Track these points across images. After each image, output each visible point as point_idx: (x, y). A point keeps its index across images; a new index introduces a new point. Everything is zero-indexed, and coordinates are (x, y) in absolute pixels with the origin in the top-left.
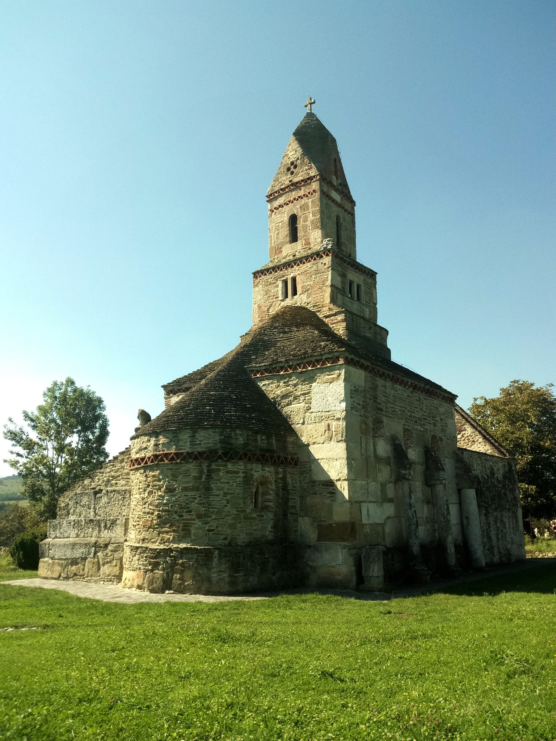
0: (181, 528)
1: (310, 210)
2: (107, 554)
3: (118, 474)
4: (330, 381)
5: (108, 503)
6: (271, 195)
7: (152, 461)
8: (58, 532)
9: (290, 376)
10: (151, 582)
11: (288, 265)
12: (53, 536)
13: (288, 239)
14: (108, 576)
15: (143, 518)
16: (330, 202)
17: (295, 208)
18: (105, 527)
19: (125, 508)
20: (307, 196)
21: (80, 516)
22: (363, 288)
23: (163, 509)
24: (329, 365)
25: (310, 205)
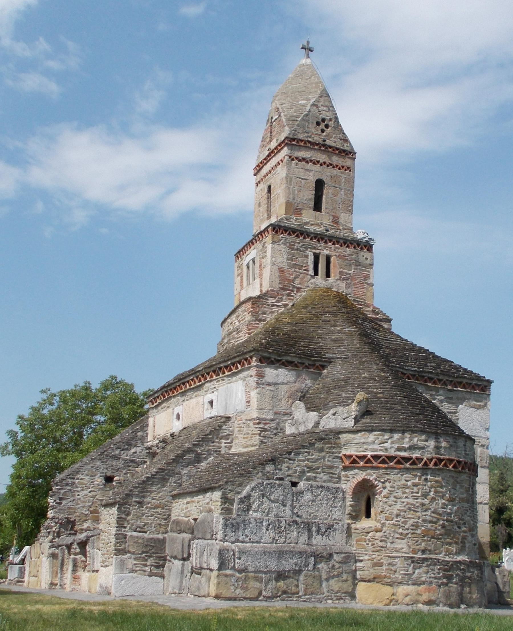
0: (460, 540)
2: (333, 566)
3: (316, 465)
4: (478, 407)
5: (313, 501)
6: (294, 140)
7: (436, 464)
8: (240, 533)
9: (437, 390)
10: (448, 596)
12: (233, 539)
14: (337, 593)
15: (422, 526)
17: (326, 174)
18: (318, 531)
19: (335, 510)
20: (339, 169)
21: (268, 514)
23: (447, 518)
24: (459, 389)
25: (343, 181)
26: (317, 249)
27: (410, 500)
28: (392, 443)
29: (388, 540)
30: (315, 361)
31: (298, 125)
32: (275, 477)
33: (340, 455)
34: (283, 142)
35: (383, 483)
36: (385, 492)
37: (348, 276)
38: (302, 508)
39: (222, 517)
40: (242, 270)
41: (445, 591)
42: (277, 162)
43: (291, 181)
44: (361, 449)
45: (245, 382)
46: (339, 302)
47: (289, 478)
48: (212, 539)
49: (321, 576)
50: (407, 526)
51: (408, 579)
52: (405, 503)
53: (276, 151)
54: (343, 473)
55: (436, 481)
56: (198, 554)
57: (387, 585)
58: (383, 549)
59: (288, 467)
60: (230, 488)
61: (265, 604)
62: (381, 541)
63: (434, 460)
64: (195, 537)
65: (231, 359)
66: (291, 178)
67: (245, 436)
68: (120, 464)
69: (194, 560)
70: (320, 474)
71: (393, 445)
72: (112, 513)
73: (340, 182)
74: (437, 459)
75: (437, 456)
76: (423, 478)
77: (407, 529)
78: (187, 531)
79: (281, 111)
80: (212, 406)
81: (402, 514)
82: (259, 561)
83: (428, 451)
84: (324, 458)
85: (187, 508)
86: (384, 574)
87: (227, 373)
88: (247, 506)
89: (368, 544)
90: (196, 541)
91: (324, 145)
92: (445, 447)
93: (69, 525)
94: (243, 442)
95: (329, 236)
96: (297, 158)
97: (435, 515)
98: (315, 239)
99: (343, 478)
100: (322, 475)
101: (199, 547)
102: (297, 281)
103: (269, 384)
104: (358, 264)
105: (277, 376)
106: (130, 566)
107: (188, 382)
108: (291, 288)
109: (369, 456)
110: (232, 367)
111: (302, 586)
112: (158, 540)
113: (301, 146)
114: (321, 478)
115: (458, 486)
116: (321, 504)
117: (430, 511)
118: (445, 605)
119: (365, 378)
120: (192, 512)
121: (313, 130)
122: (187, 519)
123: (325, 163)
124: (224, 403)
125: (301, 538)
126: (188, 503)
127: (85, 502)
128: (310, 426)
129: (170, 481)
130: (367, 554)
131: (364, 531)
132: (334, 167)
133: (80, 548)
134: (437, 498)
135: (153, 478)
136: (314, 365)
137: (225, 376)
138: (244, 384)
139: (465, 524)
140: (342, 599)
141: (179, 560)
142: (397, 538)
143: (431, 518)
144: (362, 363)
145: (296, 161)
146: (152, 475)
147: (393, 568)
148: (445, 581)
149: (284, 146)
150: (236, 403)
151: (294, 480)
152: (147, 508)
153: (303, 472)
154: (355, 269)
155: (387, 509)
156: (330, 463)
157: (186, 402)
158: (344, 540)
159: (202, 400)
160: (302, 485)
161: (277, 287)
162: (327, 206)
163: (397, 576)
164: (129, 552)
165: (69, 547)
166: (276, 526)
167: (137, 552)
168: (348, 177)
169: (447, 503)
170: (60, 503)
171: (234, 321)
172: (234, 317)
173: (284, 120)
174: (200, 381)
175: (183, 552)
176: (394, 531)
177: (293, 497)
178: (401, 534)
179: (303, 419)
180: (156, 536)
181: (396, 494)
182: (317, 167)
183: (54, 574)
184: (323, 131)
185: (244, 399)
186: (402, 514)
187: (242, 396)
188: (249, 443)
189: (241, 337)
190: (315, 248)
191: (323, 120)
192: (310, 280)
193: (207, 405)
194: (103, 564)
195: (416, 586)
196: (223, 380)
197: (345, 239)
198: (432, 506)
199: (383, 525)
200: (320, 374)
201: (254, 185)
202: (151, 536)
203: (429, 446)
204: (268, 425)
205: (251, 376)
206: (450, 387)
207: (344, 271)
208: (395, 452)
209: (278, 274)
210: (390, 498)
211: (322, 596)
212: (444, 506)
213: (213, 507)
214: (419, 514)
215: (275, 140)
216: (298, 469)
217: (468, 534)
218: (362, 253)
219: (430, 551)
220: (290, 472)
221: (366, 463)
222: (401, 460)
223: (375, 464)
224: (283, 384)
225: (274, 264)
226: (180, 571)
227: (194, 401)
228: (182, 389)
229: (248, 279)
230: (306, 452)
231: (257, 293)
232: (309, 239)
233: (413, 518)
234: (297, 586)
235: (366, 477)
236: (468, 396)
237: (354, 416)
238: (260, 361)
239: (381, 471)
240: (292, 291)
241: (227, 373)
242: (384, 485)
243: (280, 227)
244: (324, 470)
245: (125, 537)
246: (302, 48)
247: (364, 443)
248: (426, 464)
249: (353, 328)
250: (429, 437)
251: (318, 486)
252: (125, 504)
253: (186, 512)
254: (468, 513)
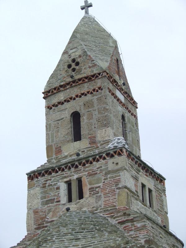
1: (96, 107)
6: (49, 92)
11: (72, 165)
13: (71, 137)
16: (115, 100)
20: (92, 93)
22: (154, 193)
25: (95, 102)
26: (68, 177)
37: (97, 190)
96: (53, 106)
108: (45, 225)
145: (53, 108)
182: (72, 102)
190: (65, 177)
191: (74, 60)
218: (112, 160)
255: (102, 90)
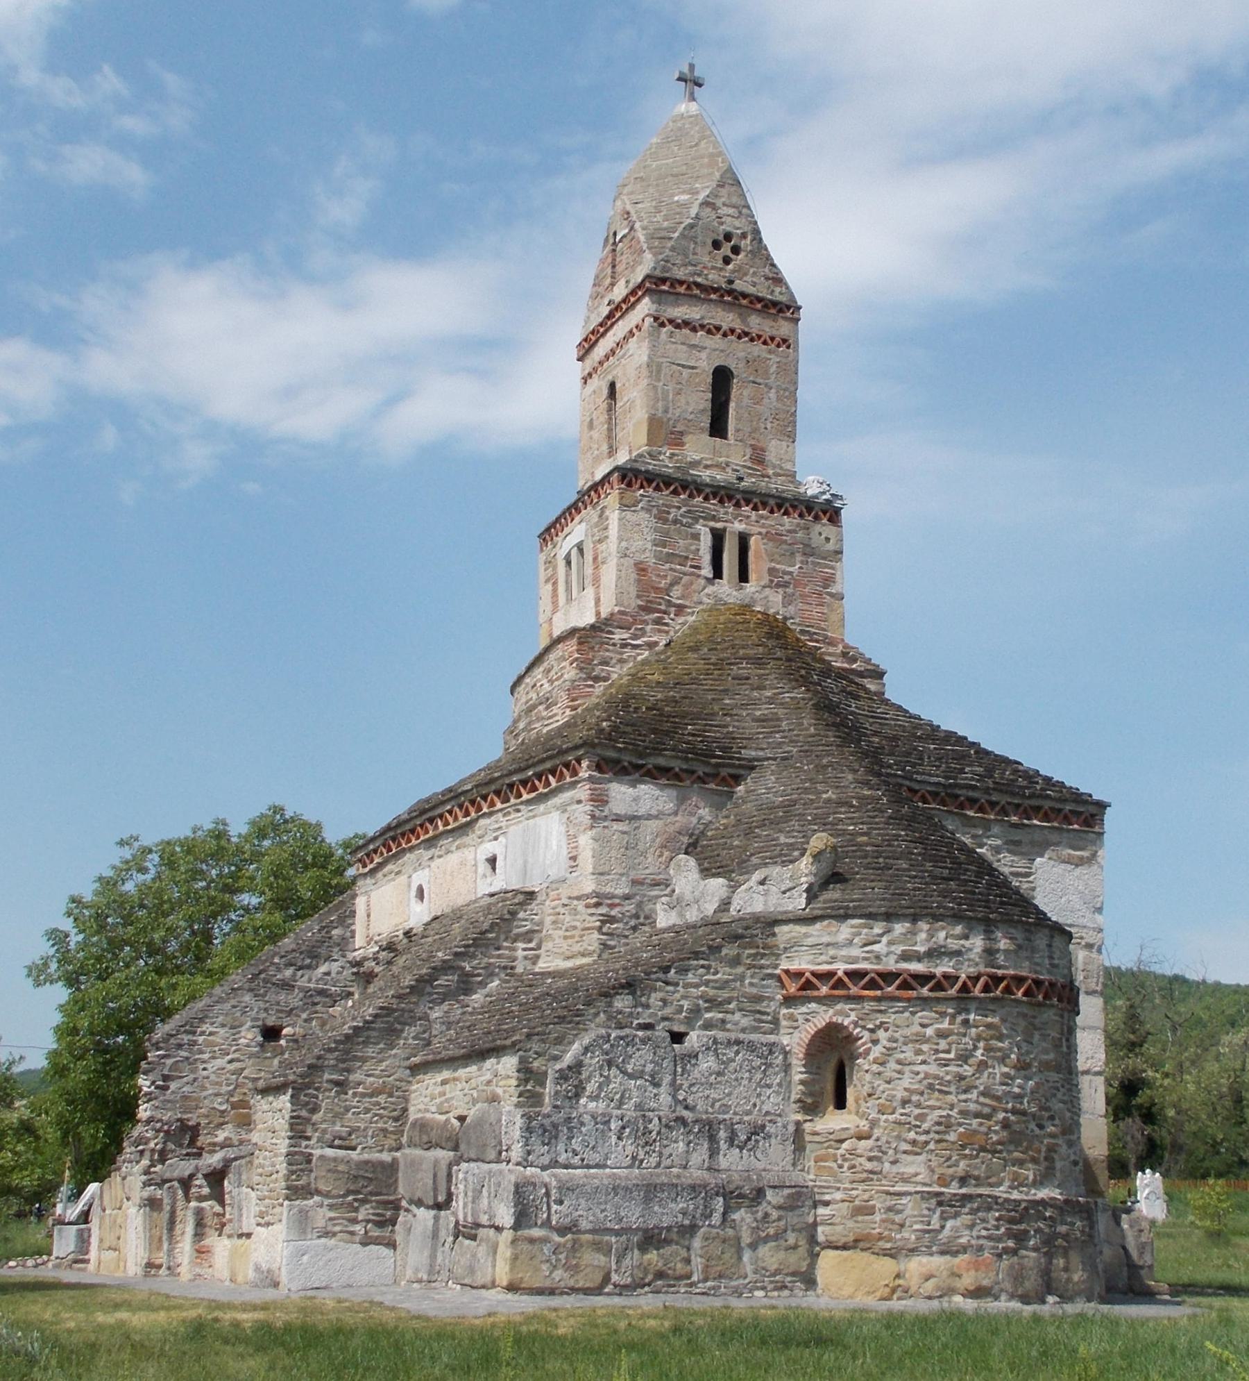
0: (1043, 1154)
2: (766, 1215)
3: (725, 994)
4: (1076, 861)
5: (719, 1074)
7: (986, 989)
8: (561, 1147)
9: (987, 825)
10: (1018, 1276)
12: (546, 1160)
13: (706, 421)
14: (774, 1275)
15: (960, 1125)
18: (731, 1141)
19: (769, 1092)
20: (765, 343)
21: (621, 1103)
23: (1013, 1107)
24: (1035, 822)
25: (773, 369)
26: (719, 520)
27: (933, 1069)
28: (890, 943)
29: (885, 1157)
30: (718, 765)
31: (673, 249)
32: (636, 1022)
33: (778, 972)
34: (639, 287)
35: (872, 1031)
36: (877, 1051)
37: (787, 578)
38: (694, 1089)
39: (520, 1112)
40: (555, 568)
41: (1011, 1267)
42: (628, 329)
43: (659, 372)
44: (823, 958)
45: (566, 815)
46: (769, 635)
47: (666, 1023)
48: (498, 1161)
49: (738, 1239)
50: (925, 1126)
51: (930, 1242)
52: (922, 1076)
53: (624, 307)
54: (784, 1011)
55: (989, 1026)
56: (470, 1194)
57: (885, 1255)
58: (875, 1177)
59: (664, 1001)
60: (536, 1047)
61: (617, 1300)
62: (870, 1159)
63: (982, 980)
64: (461, 1157)
65: (534, 765)
66: (659, 365)
67: (568, 934)
68: (295, 999)
69: (461, 1208)
70: (733, 1013)
71: (893, 948)
72: (279, 1107)
73: (766, 372)
74: (989, 976)
75: (989, 970)
76: (959, 1019)
77: (927, 1132)
78: (443, 1144)
79: (634, 218)
80: (494, 869)
81: (915, 1098)
82: (603, 1207)
83: (969, 960)
84: (742, 978)
85: (443, 1094)
86: (878, 1230)
87: (525, 797)
88: (575, 1087)
89: (841, 1167)
90: (464, 1166)
91: (730, 292)
92: (1005, 951)
93: (186, 1136)
94: (563, 947)
95: (744, 492)
96: (671, 321)
97: (987, 1101)
98: (714, 498)
99: (784, 1023)
100: (737, 1016)
101: (470, 1179)
102: (676, 592)
103: (618, 819)
104: (809, 551)
105: (636, 799)
106: (321, 1223)
107: (441, 816)
108: (663, 607)
109: (840, 973)
110: (537, 782)
111: (699, 1260)
112: (382, 1164)
113: (678, 294)
114: (736, 1024)
115: (1037, 1037)
116: (736, 1080)
117: (975, 1091)
118: (1012, 1297)
119: (829, 800)
120: (454, 1102)
121: (706, 259)
122: (443, 1118)
123: (732, 331)
124: (520, 862)
125: (695, 1155)
126: (444, 1082)
127: (219, 1084)
128: (710, 908)
129: (405, 1035)
130: (838, 1189)
131: (831, 1137)
132: (752, 340)
133: (210, 1185)
134: (990, 1062)
135: (368, 1029)
136: (716, 775)
137: (522, 803)
138: (564, 820)
139: (1052, 1118)
140: (786, 1287)
141: (428, 1207)
142: (905, 1152)
143: (979, 1108)
144: (821, 768)
145: (669, 328)
146: (366, 1022)
147: (898, 1218)
148: (1011, 1244)
149: (643, 295)
150: (548, 862)
151: (677, 1028)
152: (355, 1094)
153: (696, 1011)
154: (802, 562)
155: (881, 1088)
156: (754, 991)
157: (437, 861)
158: (790, 1158)
159: (471, 856)
160: (694, 1039)
161: (633, 605)
162: (740, 426)
163: (906, 1235)
164: (318, 1192)
165: (186, 1183)
166: (639, 1130)
167: (334, 1192)
168: (784, 360)
169: (1012, 1072)
170: (165, 1088)
171: (539, 680)
172: (538, 672)
173: (642, 238)
174: (467, 814)
175: (435, 1189)
176: (898, 1138)
177: (675, 1066)
178: (914, 1143)
179: (694, 894)
180: (376, 1156)
181: (902, 1056)
183: (154, 1243)
184: (727, 261)
185: (565, 852)
186: (915, 1098)
187: (559, 847)
188: (577, 948)
189: (555, 715)
190: (714, 518)
191: (728, 237)
192: (704, 588)
193: (483, 867)
194: (261, 1220)
195: (948, 1257)
196: (518, 811)
197: (779, 497)
198: (981, 1081)
199: (874, 1124)
200: (730, 795)
201: (579, 383)
202: (366, 1156)
203: (971, 950)
204: (617, 909)
205: (579, 802)
206: (1014, 819)
207: (778, 566)
208: (897, 962)
209: (634, 576)
210: (888, 1065)
211: (741, 1281)
212: (1007, 1079)
213: (499, 1091)
214: (952, 1098)
215: (622, 282)
216: (686, 1004)
217: (1060, 1142)
218: (817, 528)
219: (977, 1178)
220: (668, 1011)
221: (833, 988)
222: (910, 980)
223: (854, 990)
224: (649, 817)
225: (626, 555)
226: (429, 1233)
227: (454, 858)
228: (427, 832)
229: (568, 589)
230: (703, 967)
231: (589, 619)
232: (701, 499)
233: (940, 1108)
234: (688, 1261)
235: (834, 1020)
236: (1054, 837)
237: (805, 886)
238: (599, 768)
239: (868, 1006)
240: (665, 613)
241: (525, 797)
242: (874, 1037)
243: (637, 473)
244: (741, 1005)
245: (308, 1159)
246: (679, 79)
247: (828, 945)
248: (965, 988)
249: (800, 693)
250: (971, 929)
251: (729, 1042)
252: (308, 1086)
253: (442, 1103)
254: (1059, 1095)
255: (788, 347)
